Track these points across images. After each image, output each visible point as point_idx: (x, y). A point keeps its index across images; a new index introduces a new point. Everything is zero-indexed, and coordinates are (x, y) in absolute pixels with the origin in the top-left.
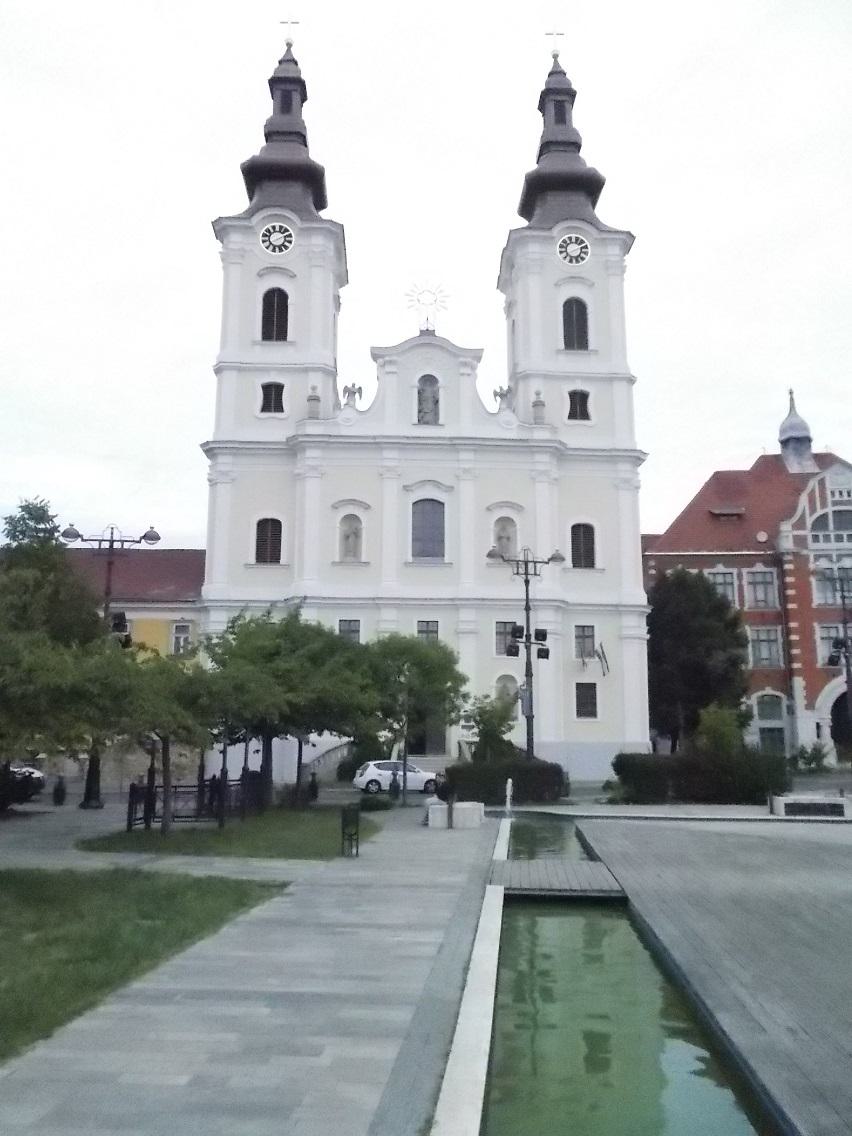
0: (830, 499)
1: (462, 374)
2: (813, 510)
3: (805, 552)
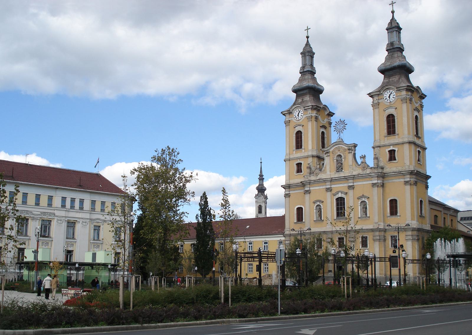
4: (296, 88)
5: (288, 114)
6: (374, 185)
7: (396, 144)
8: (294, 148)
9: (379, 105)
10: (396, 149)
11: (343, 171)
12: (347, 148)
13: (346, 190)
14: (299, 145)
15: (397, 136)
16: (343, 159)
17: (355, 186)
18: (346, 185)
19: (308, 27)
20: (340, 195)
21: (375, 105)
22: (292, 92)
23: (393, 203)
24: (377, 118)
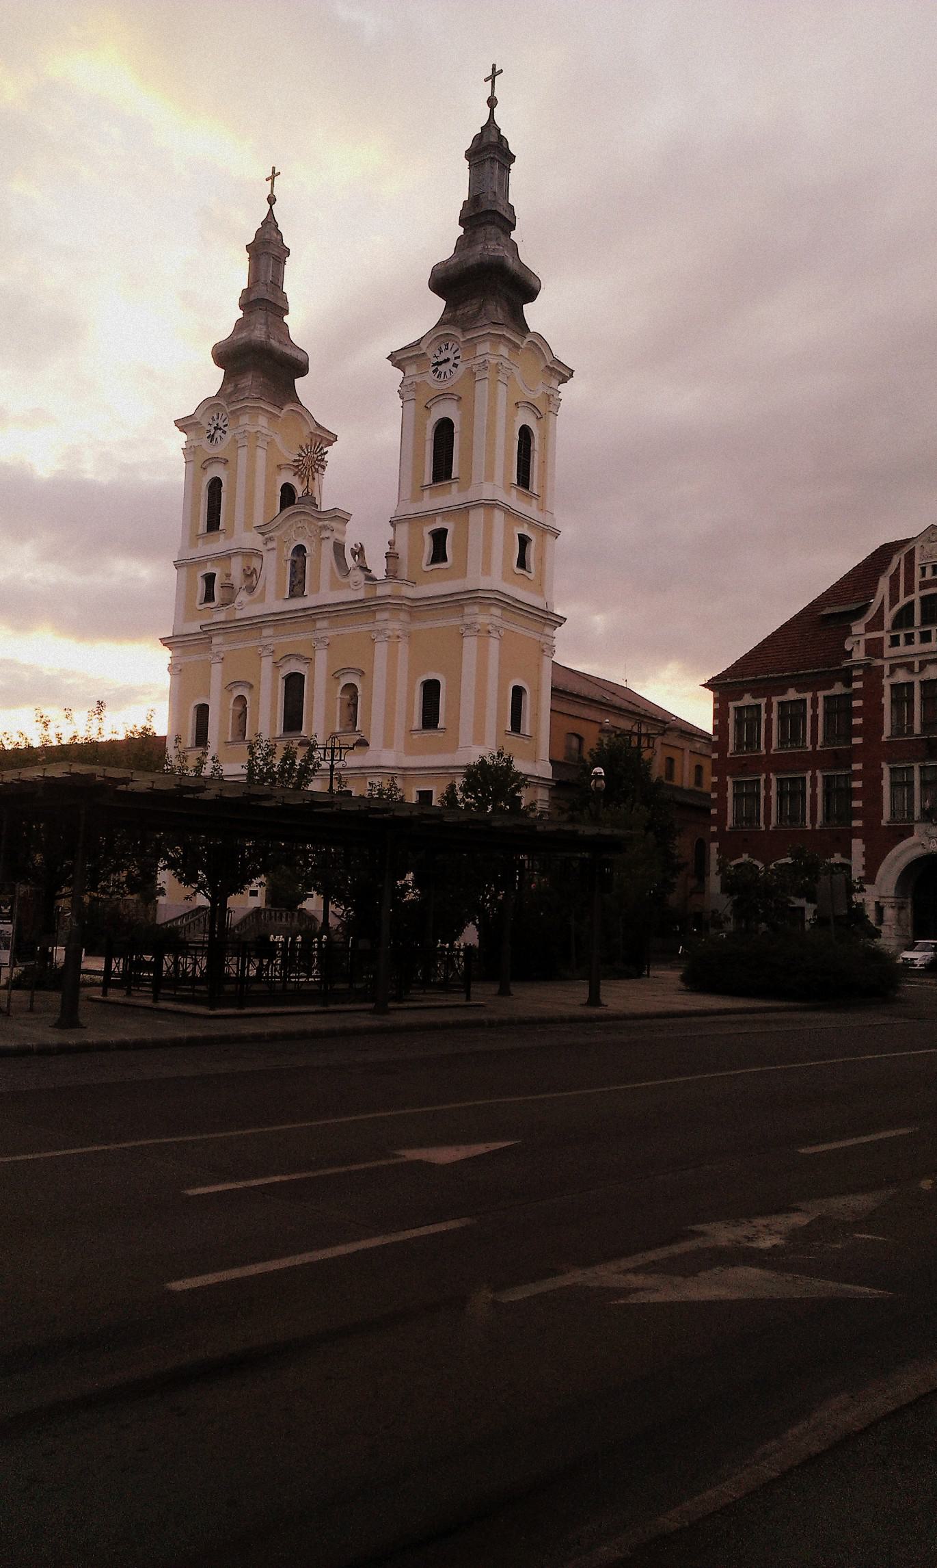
0: (918, 579)
1: (323, 539)
2: (894, 599)
3: (879, 662)
19: (274, 168)
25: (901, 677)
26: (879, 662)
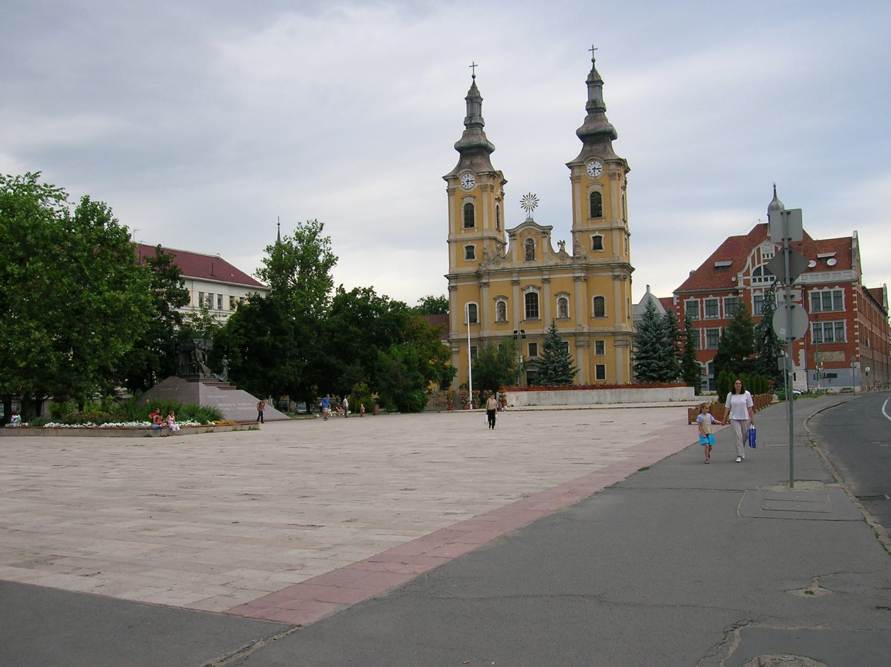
0: (762, 259)
2: (754, 265)
3: (748, 288)
4: (462, 145)
5: (453, 180)
6: (577, 279)
7: (603, 230)
8: (463, 226)
9: (454, 191)
10: (603, 236)
11: (535, 259)
12: (541, 231)
13: (540, 285)
14: (469, 222)
15: (603, 220)
16: (535, 245)
17: (551, 280)
18: (539, 277)
20: (531, 290)
21: (574, 179)
22: (454, 149)
23: (599, 300)
24: (578, 194)
25: (758, 293)
26: (748, 288)
